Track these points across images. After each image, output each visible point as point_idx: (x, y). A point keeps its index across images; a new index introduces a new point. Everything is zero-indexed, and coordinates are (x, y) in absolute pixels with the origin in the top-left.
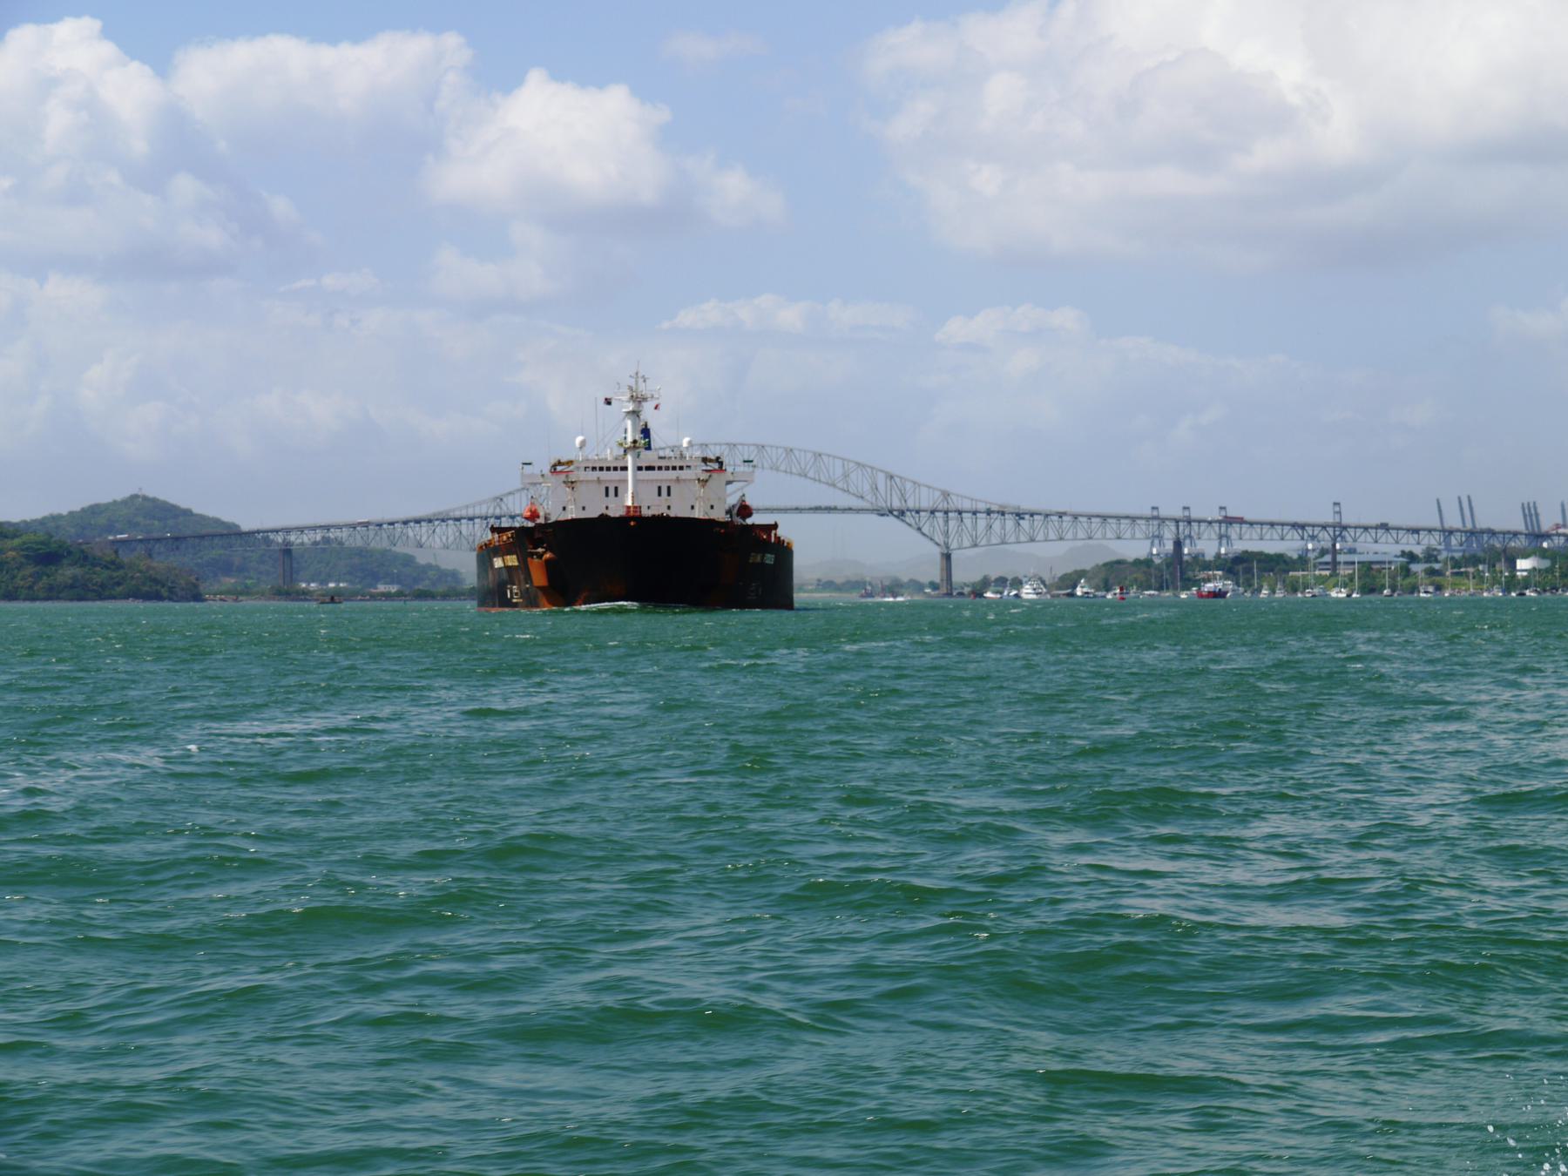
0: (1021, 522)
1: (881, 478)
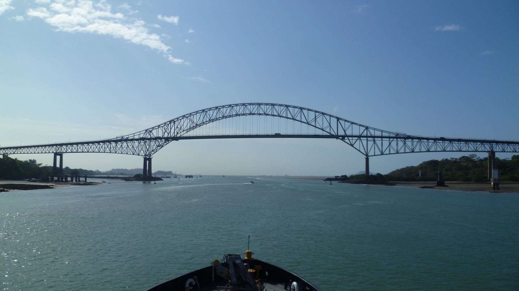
1: (334, 121)
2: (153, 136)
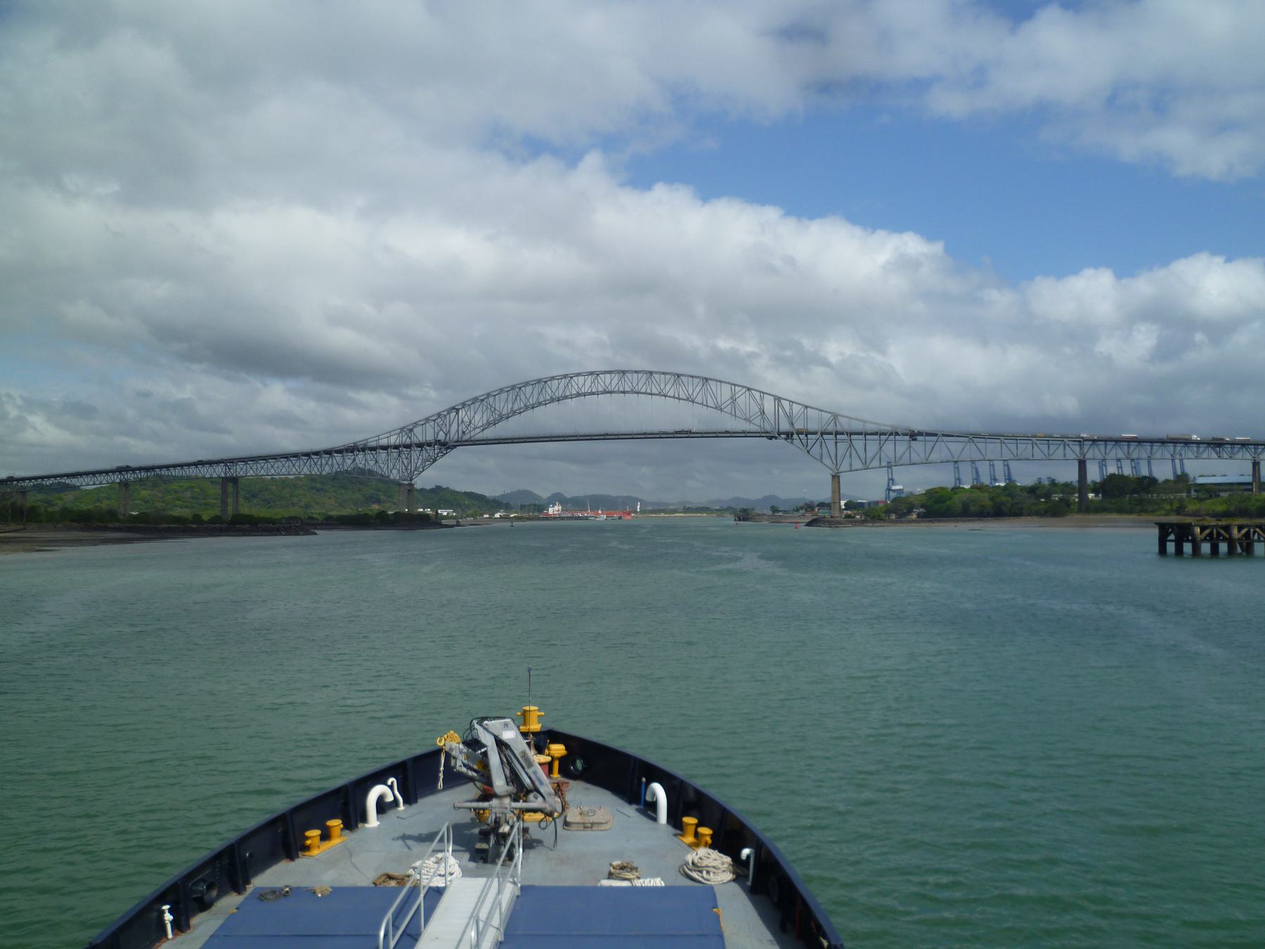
2: (415, 440)
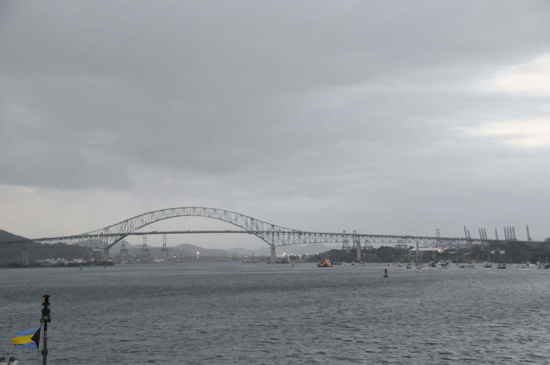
0: (301, 236)
1: (249, 220)
